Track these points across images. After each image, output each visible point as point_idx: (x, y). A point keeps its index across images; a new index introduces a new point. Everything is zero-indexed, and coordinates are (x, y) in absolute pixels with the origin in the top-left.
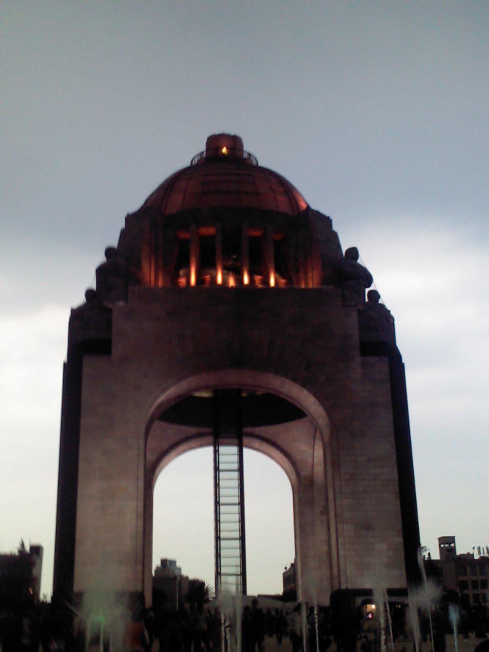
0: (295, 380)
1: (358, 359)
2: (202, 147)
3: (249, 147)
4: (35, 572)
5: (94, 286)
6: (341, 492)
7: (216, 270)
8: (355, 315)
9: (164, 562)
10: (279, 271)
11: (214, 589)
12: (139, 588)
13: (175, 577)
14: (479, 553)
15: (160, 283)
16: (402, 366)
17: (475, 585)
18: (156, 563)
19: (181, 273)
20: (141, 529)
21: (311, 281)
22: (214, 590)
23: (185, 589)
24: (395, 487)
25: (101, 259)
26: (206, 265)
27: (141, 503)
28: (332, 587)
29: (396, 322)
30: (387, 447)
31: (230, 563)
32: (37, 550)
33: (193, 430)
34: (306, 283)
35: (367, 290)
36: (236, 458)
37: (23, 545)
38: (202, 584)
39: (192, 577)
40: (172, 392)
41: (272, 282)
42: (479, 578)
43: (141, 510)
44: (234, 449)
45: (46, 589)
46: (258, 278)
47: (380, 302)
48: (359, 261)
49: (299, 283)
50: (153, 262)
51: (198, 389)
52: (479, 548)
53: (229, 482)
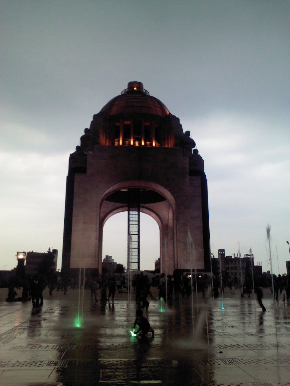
0: (162, 185)
1: (188, 177)
2: (126, 87)
3: (145, 87)
4: (54, 260)
5: (80, 145)
6: (179, 231)
7: (131, 139)
8: (188, 159)
9: (107, 257)
10: (157, 140)
11: (127, 267)
12: (96, 267)
13: (111, 263)
14: (234, 256)
15: (107, 144)
16: (206, 180)
17: (232, 268)
18: (104, 257)
19: (116, 140)
20: (98, 244)
21: (170, 144)
22: (126, 268)
23: (115, 268)
24: (201, 229)
25: (83, 133)
26: (126, 138)
27: (98, 233)
28: (174, 268)
29: (204, 162)
30: (198, 213)
31: (134, 258)
32: (55, 251)
33: (119, 205)
34: (168, 145)
35: (193, 149)
36: (137, 216)
37: (49, 249)
38: (122, 266)
39: (118, 263)
40: (111, 189)
41: (154, 145)
42: (233, 266)
43: (98, 236)
44: (137, 213)
45: (59, 267)
46: (148, 143)
47: (198, 154)
48: (190, 137)
49: (165, 145)
50: (104, 135)
51: (122, 188)
52: (234, 254)
53: (134, 225)
